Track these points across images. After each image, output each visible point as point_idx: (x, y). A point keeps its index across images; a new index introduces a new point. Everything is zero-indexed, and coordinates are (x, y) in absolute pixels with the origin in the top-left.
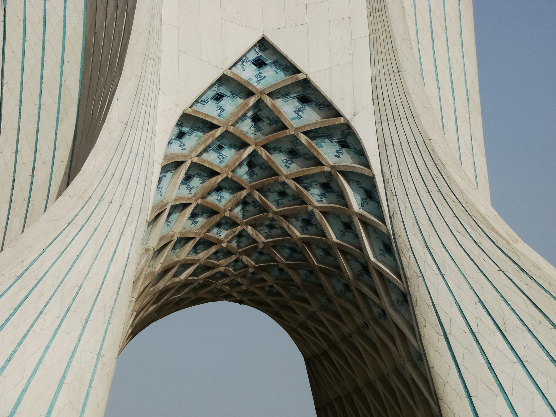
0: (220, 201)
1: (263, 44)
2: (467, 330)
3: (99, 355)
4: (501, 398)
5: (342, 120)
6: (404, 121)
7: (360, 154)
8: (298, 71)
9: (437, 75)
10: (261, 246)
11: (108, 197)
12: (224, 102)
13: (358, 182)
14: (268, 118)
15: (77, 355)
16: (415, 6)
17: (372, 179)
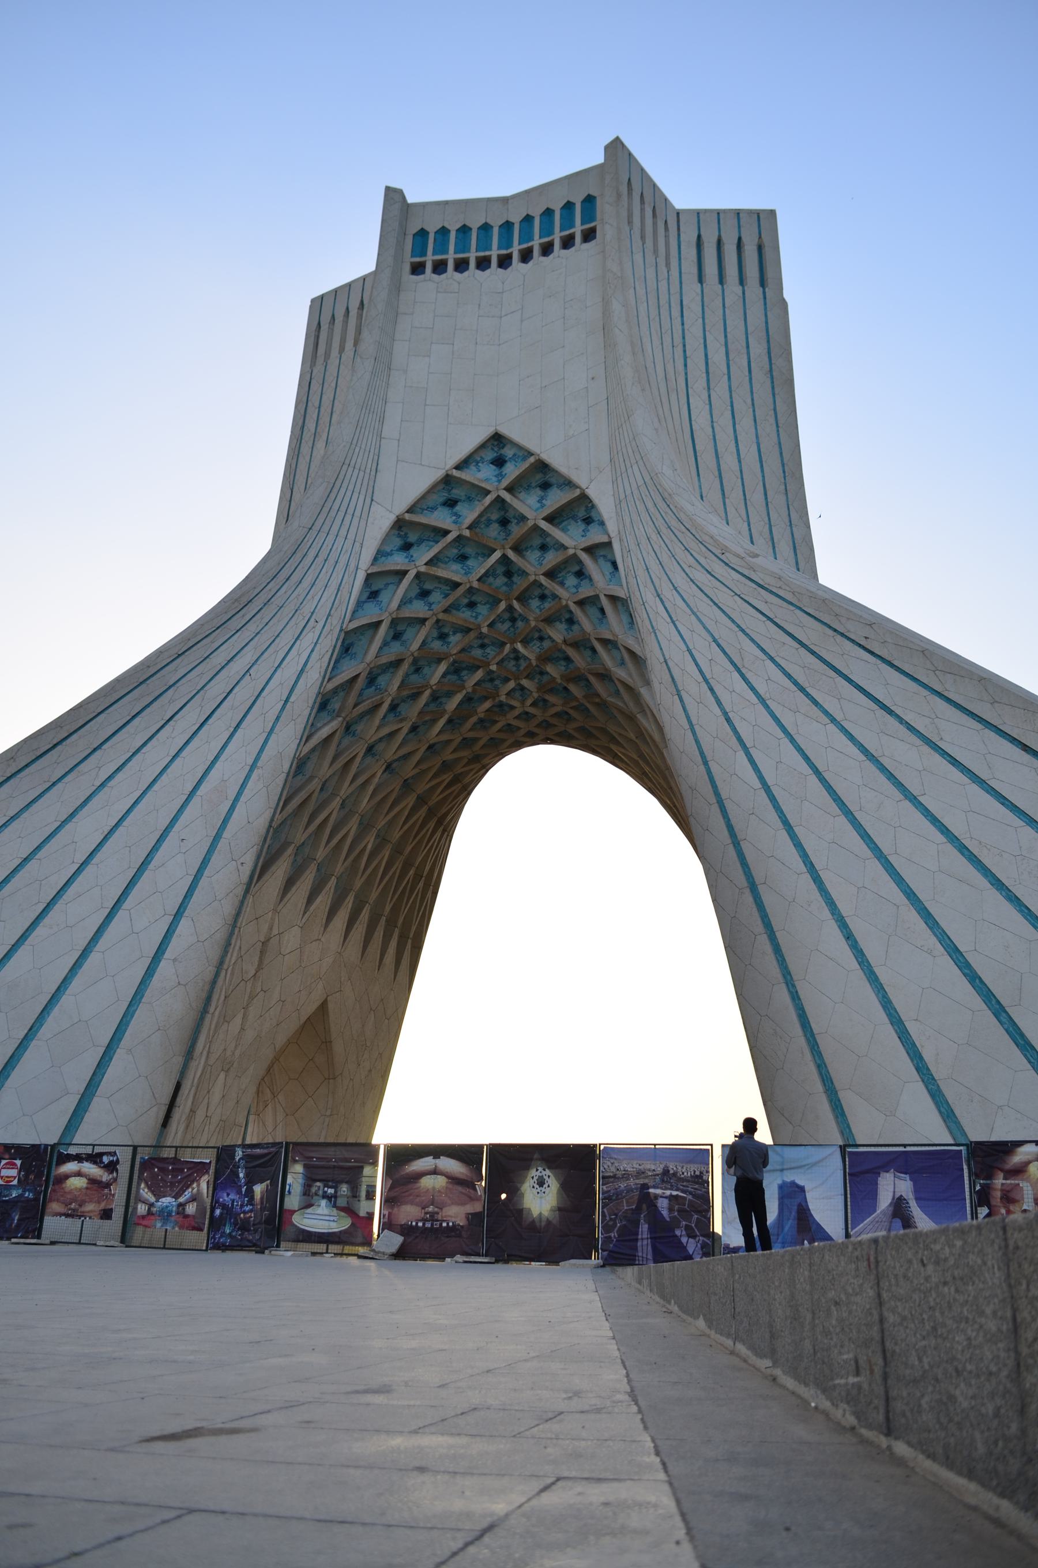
0: (476, 617)
1: (497, 439)
2: (701, 679)
3: (253, 767)
4: (741, 755)
5: (578, 492)
6: (635, 467)
7: (602, 523)
8: (531, 454)
9: (738, 450)
10: (534, 664)
11: (278, 601)
12: (458, 508)
13: (604, 556)
14: (514, 517)
15: (218, 765)
16: (709, 389)
17: (609, 544)
